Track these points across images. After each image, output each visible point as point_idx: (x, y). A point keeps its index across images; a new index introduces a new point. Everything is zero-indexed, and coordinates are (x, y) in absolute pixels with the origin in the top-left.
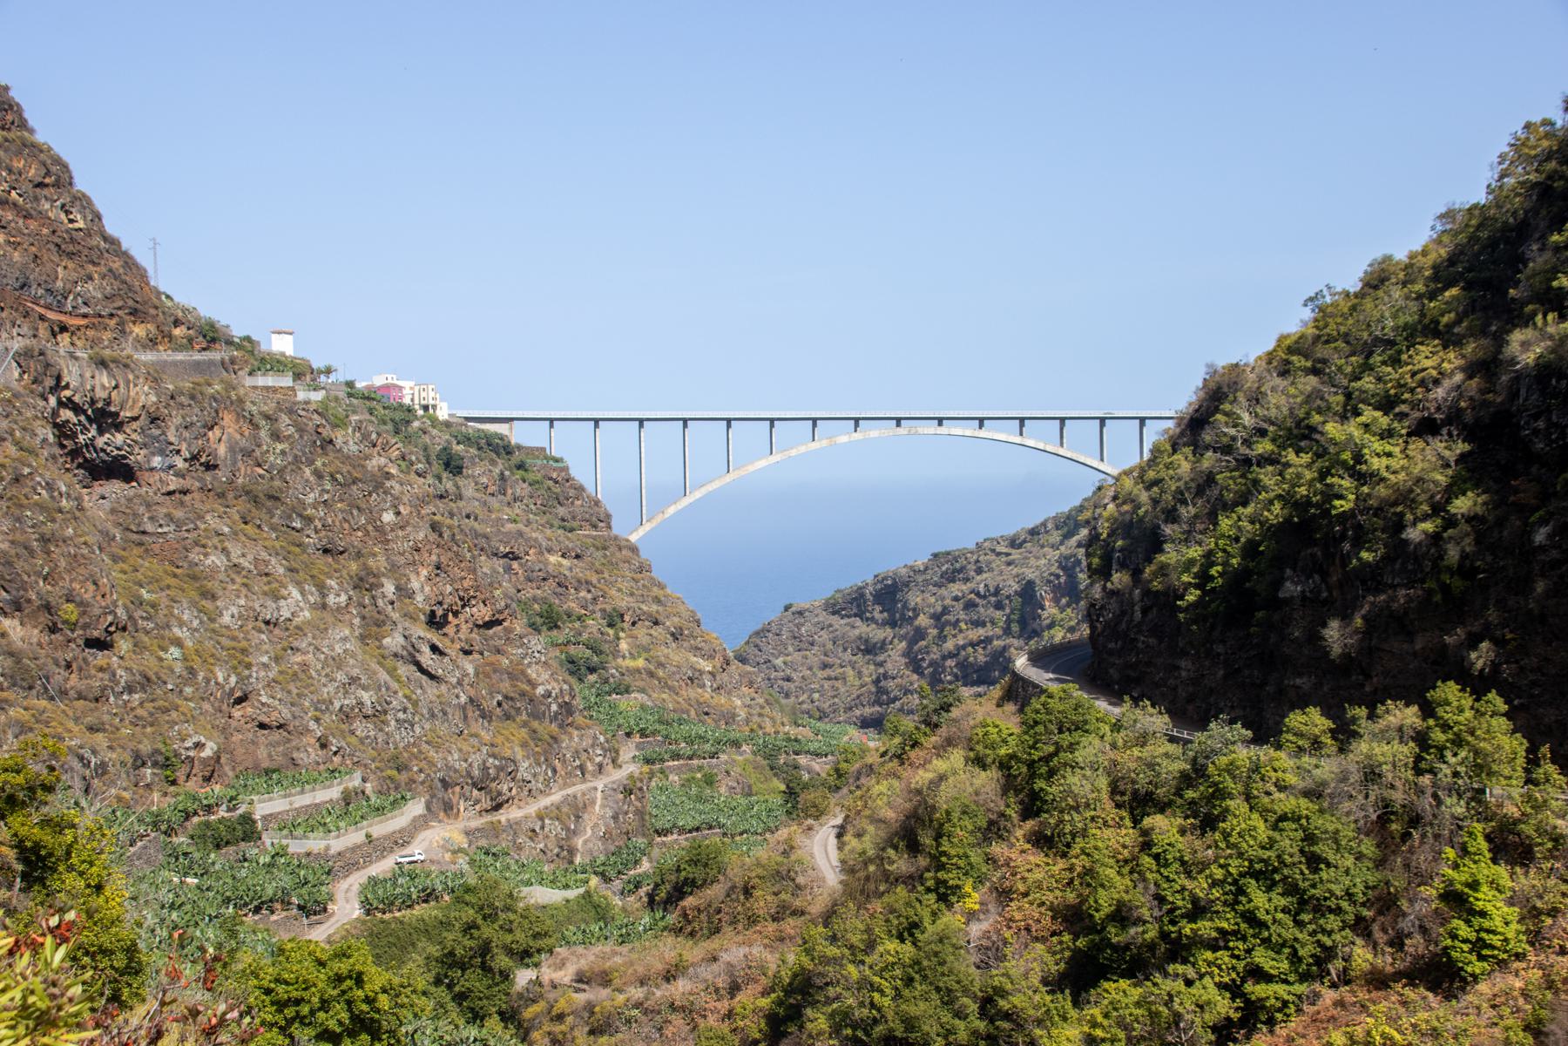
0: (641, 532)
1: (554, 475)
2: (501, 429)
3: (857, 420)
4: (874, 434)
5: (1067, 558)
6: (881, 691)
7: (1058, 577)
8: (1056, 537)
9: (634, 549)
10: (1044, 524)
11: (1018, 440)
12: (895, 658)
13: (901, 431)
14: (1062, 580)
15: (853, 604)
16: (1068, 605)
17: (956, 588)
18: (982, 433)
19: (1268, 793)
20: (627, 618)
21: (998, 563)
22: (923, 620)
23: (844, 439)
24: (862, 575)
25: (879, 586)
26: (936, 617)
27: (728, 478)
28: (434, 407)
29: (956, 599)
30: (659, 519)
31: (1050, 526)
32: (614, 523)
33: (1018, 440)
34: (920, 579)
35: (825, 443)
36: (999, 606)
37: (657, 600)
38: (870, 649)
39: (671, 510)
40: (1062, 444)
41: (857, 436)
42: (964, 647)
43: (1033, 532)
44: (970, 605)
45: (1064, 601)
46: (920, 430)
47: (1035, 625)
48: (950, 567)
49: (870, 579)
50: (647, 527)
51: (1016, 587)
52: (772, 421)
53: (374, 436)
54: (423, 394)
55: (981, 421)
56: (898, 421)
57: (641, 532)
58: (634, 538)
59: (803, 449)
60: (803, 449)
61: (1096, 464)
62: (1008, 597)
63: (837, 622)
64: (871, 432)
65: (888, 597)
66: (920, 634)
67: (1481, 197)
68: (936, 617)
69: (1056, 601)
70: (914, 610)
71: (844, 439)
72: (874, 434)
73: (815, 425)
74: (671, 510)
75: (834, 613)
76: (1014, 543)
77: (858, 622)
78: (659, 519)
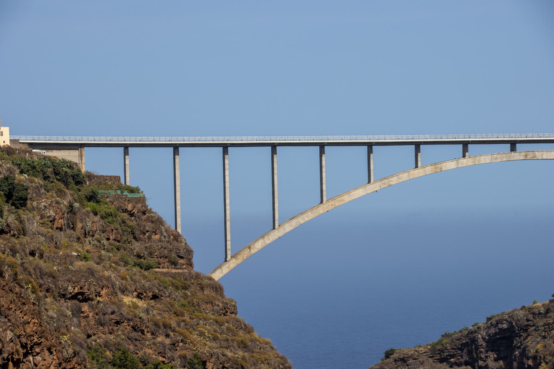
0: (225, 269)
1: (130, 207)
2: (71, 156)
3: (465, 144)
4: (485, 159)
9: (217, 288)
13: (516, 156)
23: (451, 165)
24: (473, 316)
25: (492, 331)
27: (321, 210)
30: (245, 254)
32: (195, 260)
34: (541, 322)
35: (429, 170)
37: (243, 345)
39: (259, 245)
41: (466, 162)
46: (539, 155)
49: (482, 322)
50: (232, 264)
52: (370, 146)
56: (513, 145)
57: (225, 269)
58: (217, 276)
59: (404, 177)
60: (404, 177)
64: (484, 158)
70: (535, 358)
71: (451, 165)
72: (485, 159)
73: (417, 150)
74: (259, 245)
75: (442, 361)
78: (245, 254)
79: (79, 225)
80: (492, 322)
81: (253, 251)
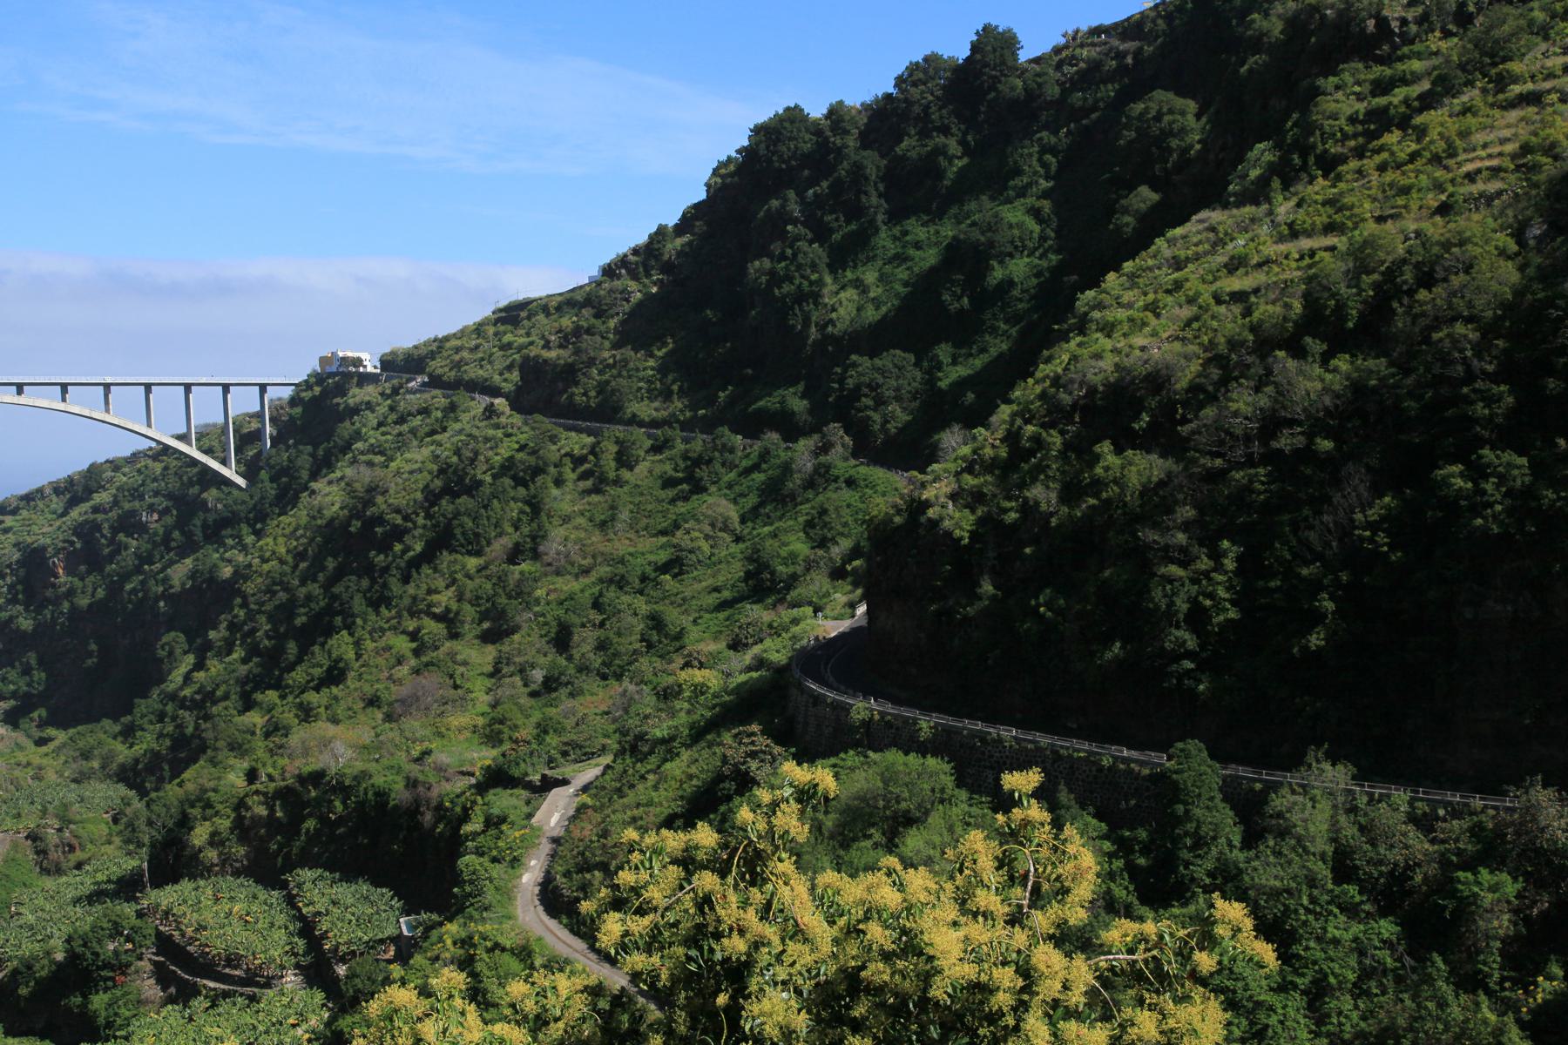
5: (81, 525)
7: (72, 543)
8: (57, 504)
10: (40, 491)
11: (62, 406)
14: (78, 546)
16: (89, 573)
18: (22, 400)
31: (47, 491)
33: (62, 406)
40: (107, 411)
43: (28, 498)
45: (83, 568)
47: (49, 593)
51: (17, 556)
55: (20, 388)
61: (144, 430)
62: (9, 566)
67: (746, 143)
69: (70, 571)
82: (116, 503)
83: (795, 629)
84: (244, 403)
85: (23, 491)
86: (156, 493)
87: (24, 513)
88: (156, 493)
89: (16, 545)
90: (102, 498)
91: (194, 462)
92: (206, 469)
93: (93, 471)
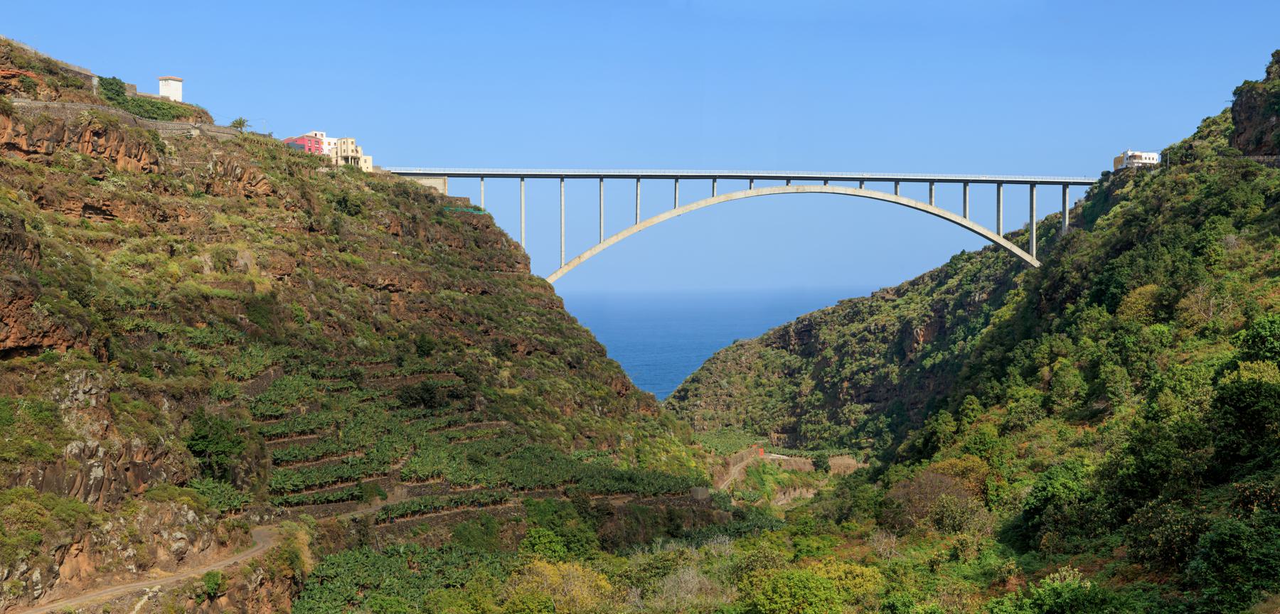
0: (559, 274)
1: (475, 222)
2: (426, 182)
4: (766, 191)
6: (796, 406)
10: (922, 277)
12: (807, 383)
15: (782, 339)
17: (856, 327)
19: (1119, 591)
20: (521, 348)
21: (887, 307)
22: (829, 352)
23: (740, 195)
24: (789, 319)
26: (838, 349)
28: (356, 159)
29: (854, 335)
30: (576, 262)
31: (927, 279)
32: (532, 266)
33: (893, 198)
36: (884, 340)
37: (560, 332)
38: (791, 373)
39: (587, 255)
40: (931, 203)
41: (752, 192)
42: (857, 373)
43: (913, 283)
44: (863, 340)
48: (853, 311)
49: (793, 322)
50: (565, 270)
53: (238, 171)
54: (344, 147)
57: (559, 274)
58: (550, 280)
59: (702, 204)
60: (702, 204)
63: (770, 352)
65: (802, 337)
66: (826, 361)
68: (838, 349)
70: (824, 343)
71: (740, 195)
72: (766, 191)
74: (587, 255)
76: (899, 292)
77: (784, 353)
78: (576, 262)
79: (422, 233)
80: (799, 321)
81: (583, 260)
82: (960, 285)
83: (224, 277)
84: (1048, 204)
85: (912, 278)
86: (987, 278)
87: (910, 294)
88: (987, 278)
89: (899, 318)
90: (952, 282)
91: (1012, 254)
92: (1021, 259)
93: (955, 259)
